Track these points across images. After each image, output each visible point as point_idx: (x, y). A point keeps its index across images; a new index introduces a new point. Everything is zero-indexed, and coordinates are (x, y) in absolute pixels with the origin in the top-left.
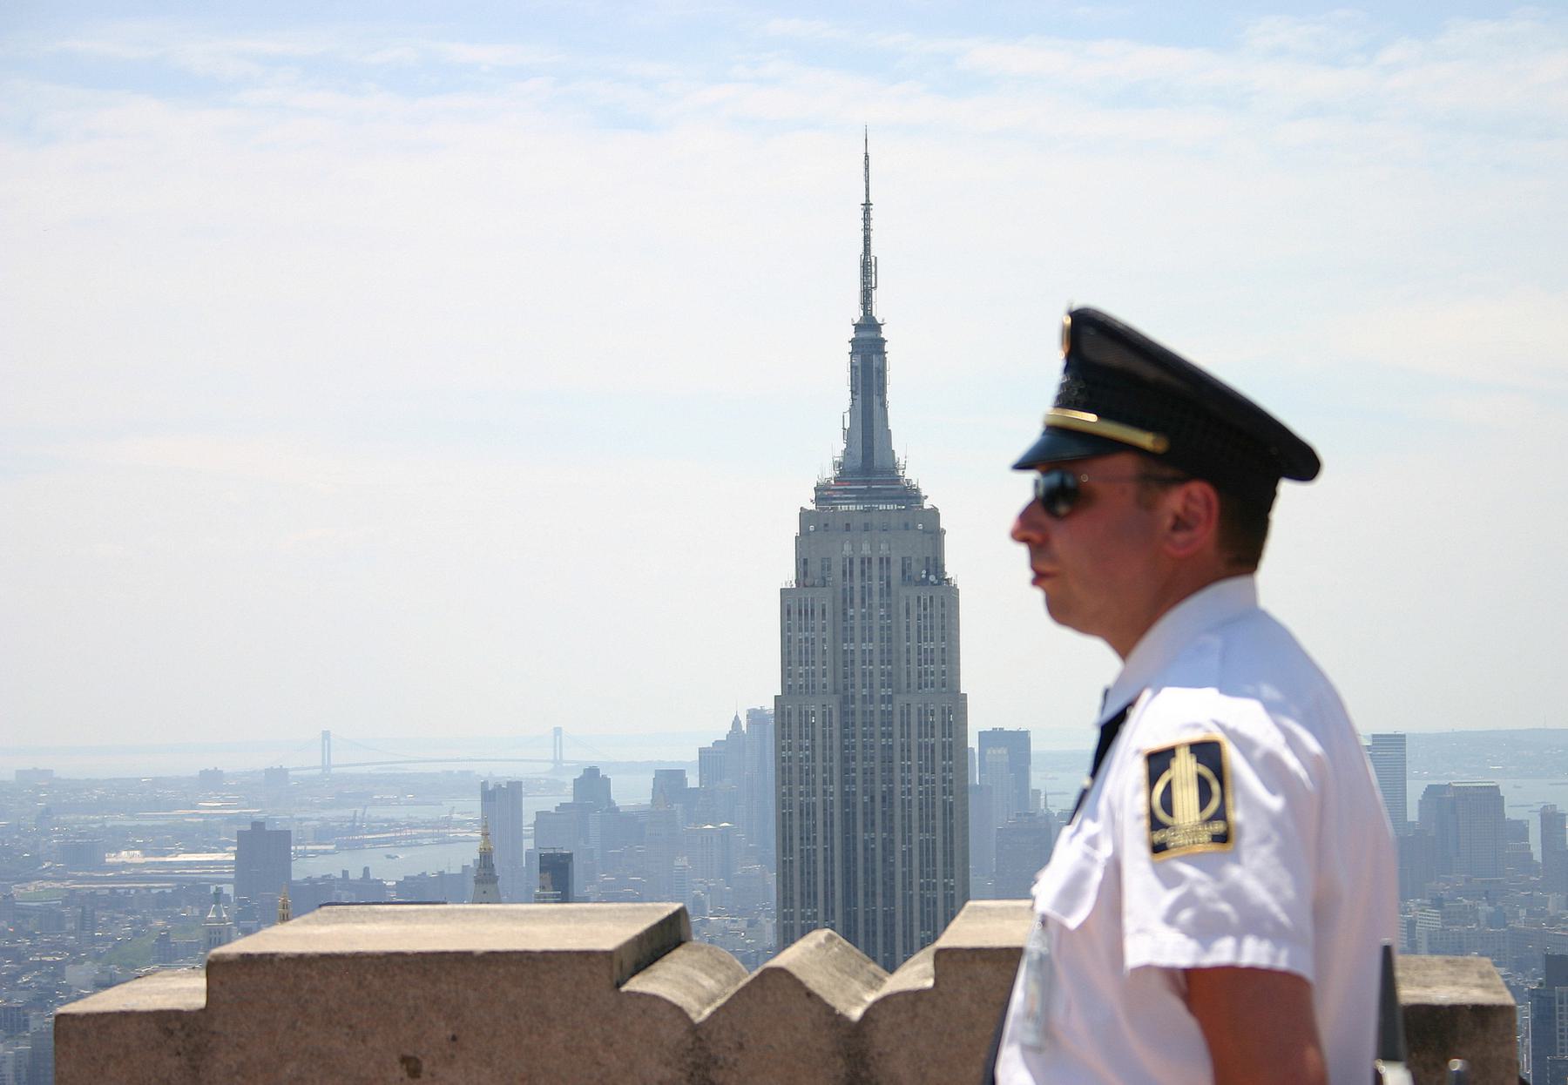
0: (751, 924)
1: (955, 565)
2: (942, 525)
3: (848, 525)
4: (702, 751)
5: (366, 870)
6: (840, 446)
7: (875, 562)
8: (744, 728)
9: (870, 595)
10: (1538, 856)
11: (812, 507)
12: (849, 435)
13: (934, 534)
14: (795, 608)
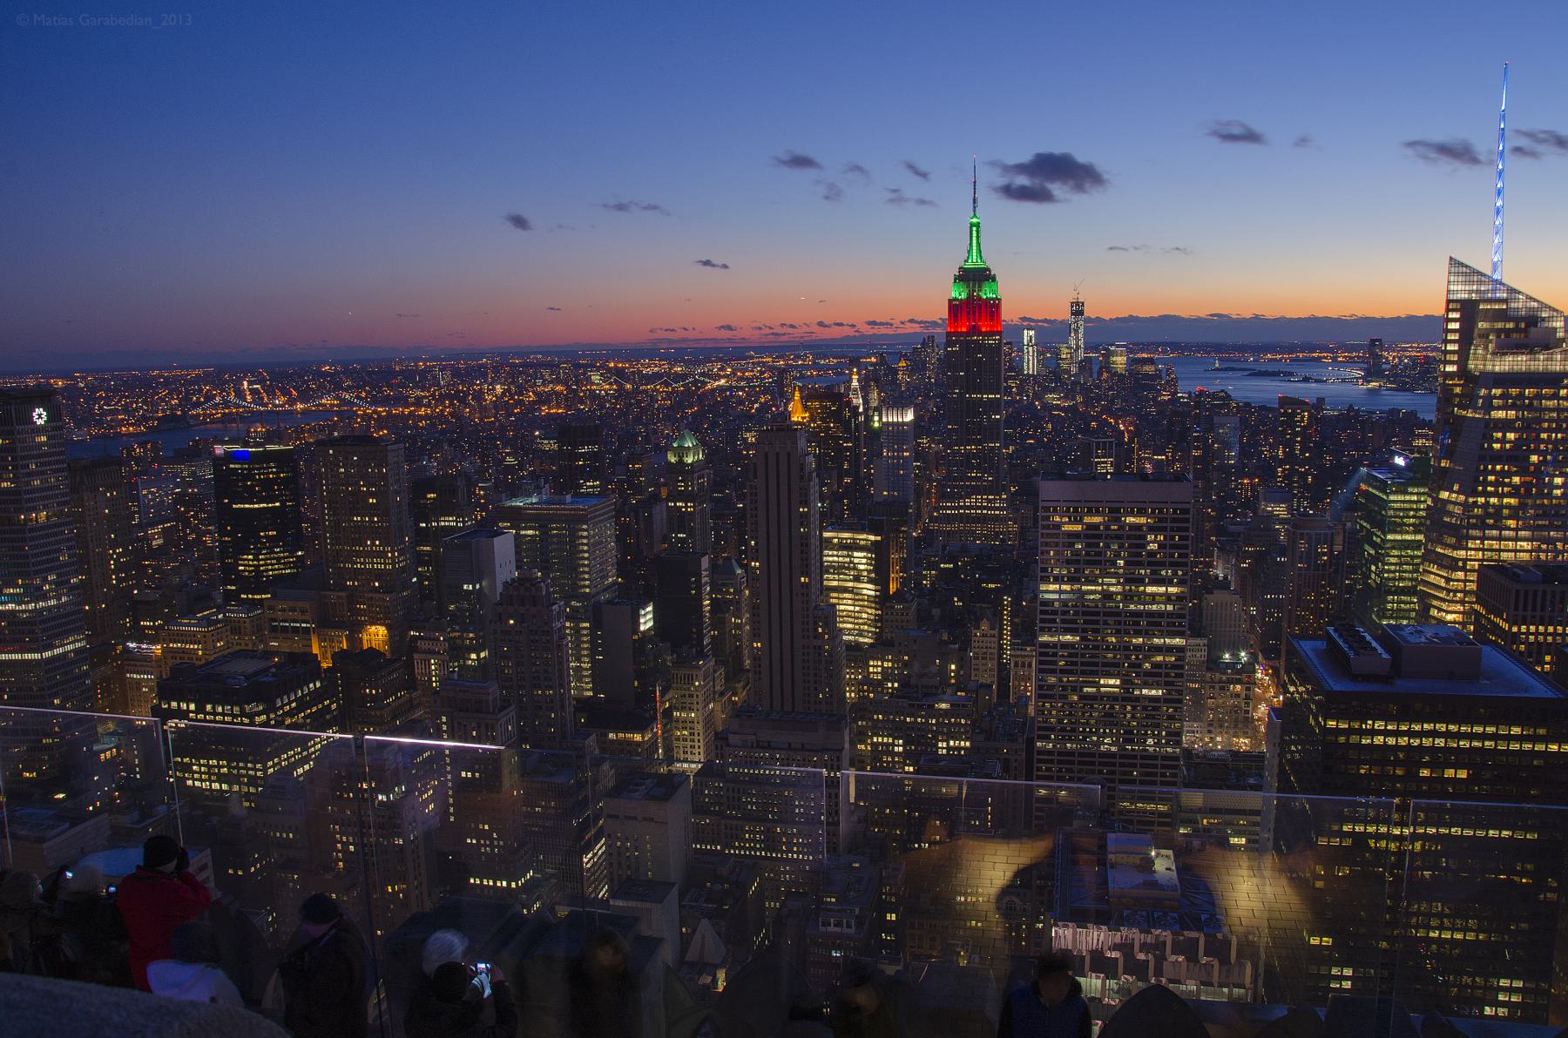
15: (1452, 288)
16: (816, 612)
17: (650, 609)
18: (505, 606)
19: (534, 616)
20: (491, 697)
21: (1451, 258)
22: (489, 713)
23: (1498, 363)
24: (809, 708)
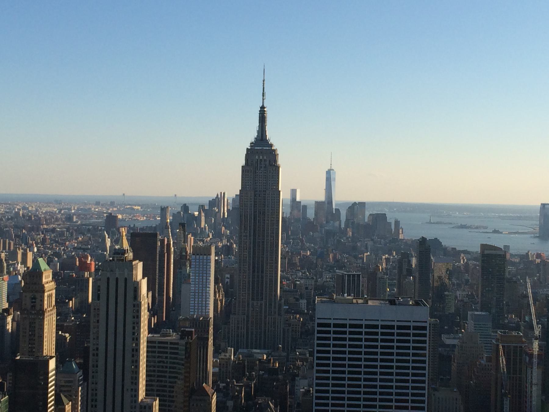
0: (221, 240)
1: (281, 161)
2: (278, 152)
3: (257, 152)
4: (209, 201)
5: (134, 225)
6: (256, 134)
7: (263, 161)
8: (219, 196)
9: (262, 168)
10: (393, 230)
11: (249, 148)
12: (258, 132)
14: (244, 170)
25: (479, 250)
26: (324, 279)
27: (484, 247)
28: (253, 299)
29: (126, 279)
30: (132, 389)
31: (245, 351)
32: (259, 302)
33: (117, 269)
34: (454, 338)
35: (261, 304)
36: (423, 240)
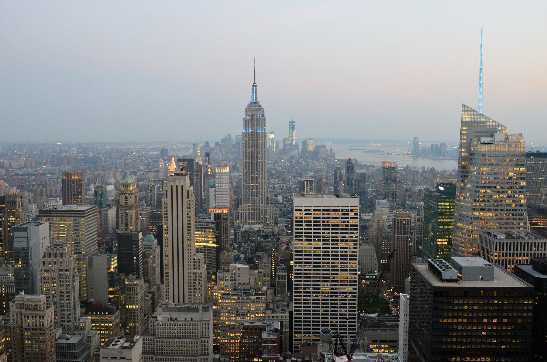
13: (263, 111)
15: (463, 116)
16: (194, 257)
17: (116, 258)
18: (46, 258)
19: (61, 263)
20: (42, 303)
21: (463, 104)
22: (40, 310)
23: (483, 148)
24: (191, 302)
25: (381, 165)
26: (291, 184)
27: (384, 163)
28: (252, 196)
29: (182, 186)
30: (188, 249)
31: (248, 226)
32: (255, 198)
33: (177, 180)
34: (368, 216)
35: (257, 199)
36: (350, 159)
